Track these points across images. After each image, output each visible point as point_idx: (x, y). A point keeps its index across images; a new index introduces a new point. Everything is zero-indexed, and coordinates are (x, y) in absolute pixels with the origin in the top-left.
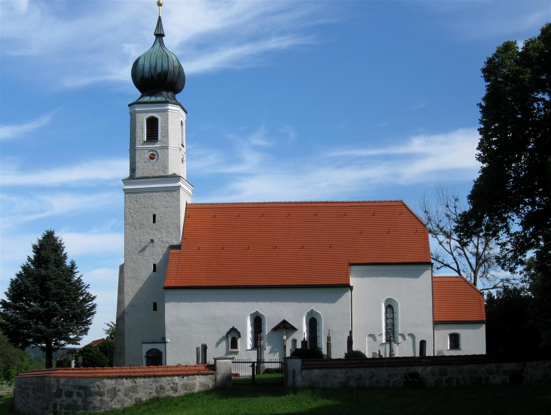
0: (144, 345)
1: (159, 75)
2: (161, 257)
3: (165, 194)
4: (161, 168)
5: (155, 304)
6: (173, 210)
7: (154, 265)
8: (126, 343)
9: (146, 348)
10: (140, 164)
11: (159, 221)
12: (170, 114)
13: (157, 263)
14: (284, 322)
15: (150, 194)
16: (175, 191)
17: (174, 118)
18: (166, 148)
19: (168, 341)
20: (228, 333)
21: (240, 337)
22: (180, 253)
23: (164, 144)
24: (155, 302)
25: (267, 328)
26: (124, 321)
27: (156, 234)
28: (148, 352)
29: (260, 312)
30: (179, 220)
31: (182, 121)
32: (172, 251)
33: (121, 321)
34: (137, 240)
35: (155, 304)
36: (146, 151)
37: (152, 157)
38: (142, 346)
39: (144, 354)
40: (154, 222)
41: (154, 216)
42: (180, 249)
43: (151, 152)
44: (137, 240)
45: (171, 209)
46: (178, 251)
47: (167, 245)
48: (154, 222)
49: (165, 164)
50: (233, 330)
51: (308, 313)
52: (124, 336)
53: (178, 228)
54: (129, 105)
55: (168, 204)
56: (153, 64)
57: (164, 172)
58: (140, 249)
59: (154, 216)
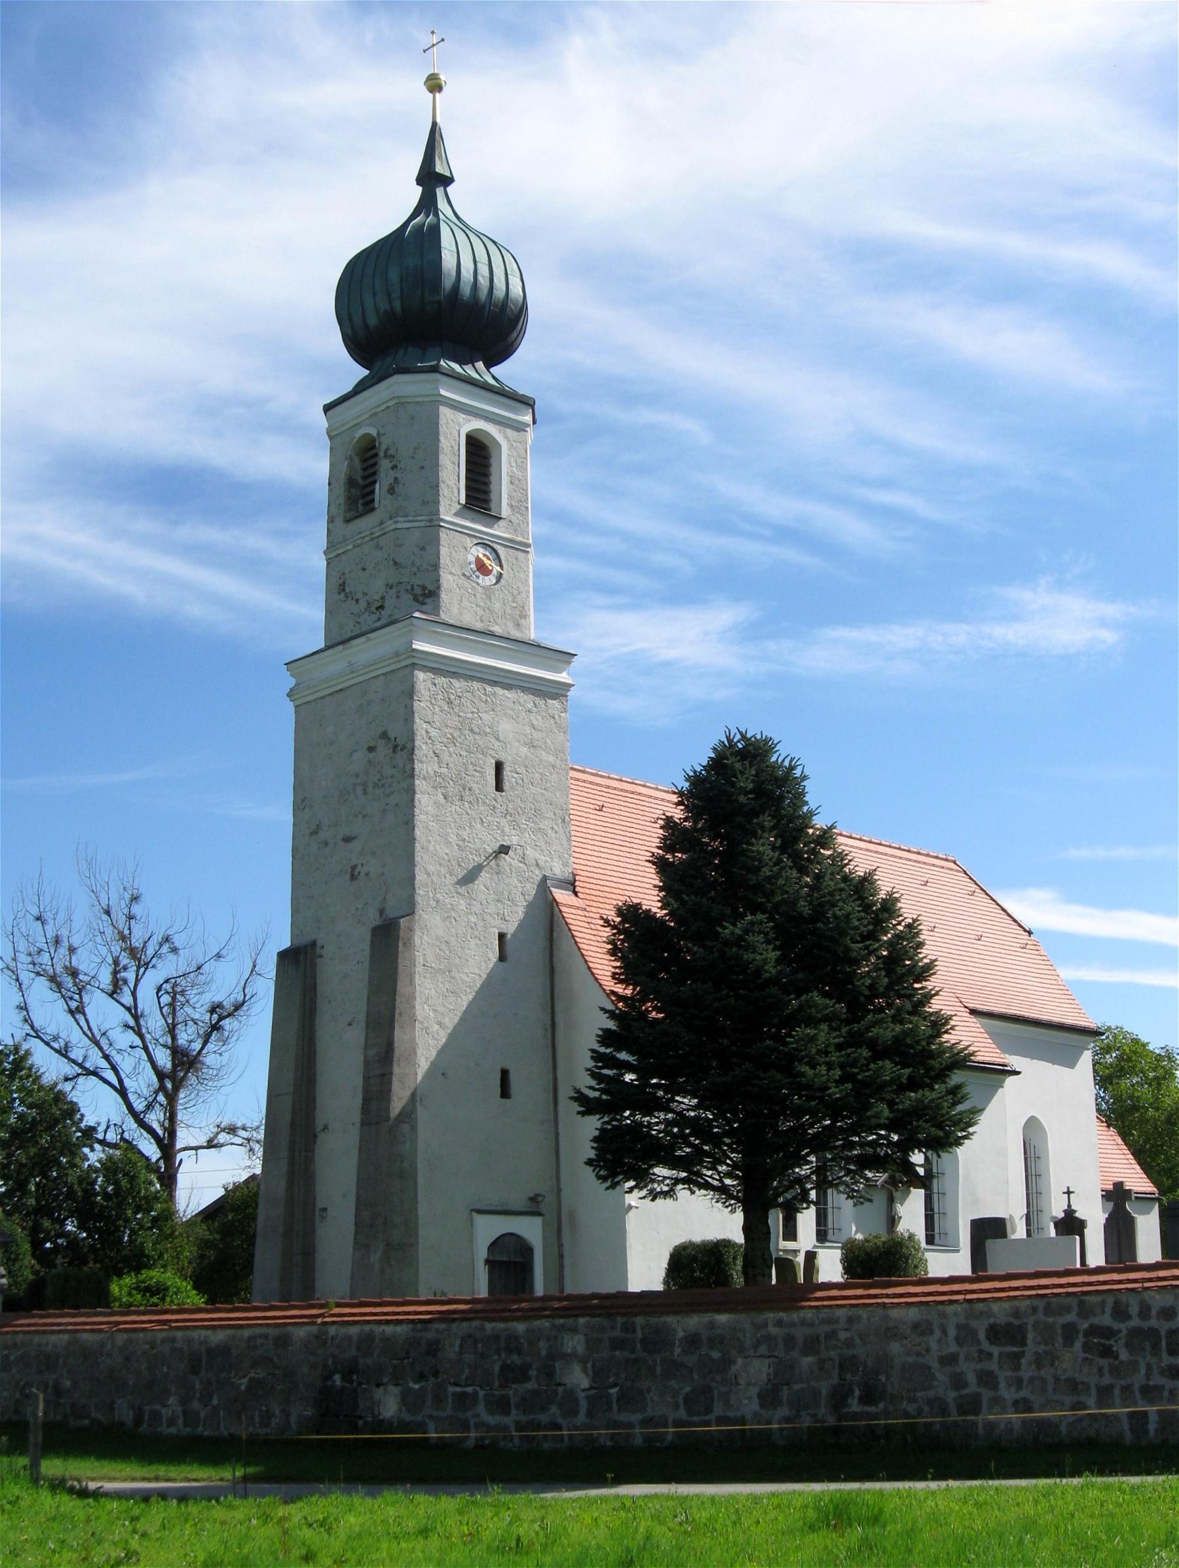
0: (480, 1220)
2: (520, 912)
3: (528, 700)
4: (508, 610)
6: (551, 759)
7: (502, 936)
8: (423, 1210)
9: (488, 1229)
10: (450, 577)
13: (510, 929)
15: (489, 688)
16: (555, 697)
24: (508, 1067)
26: (414, 1128)
27: (507, 830)
28: (494, 1246)
33: (406, 1127)
34: (453, 838)
36: (469, 542)
39: (482, 1253)
40: (499, 787)
41: (499, 767)
44: (453, 838)
48: (499, 787)
52: (416, 1183)
55: (536, 735)
58: (461, 873)
59: (499, 767)
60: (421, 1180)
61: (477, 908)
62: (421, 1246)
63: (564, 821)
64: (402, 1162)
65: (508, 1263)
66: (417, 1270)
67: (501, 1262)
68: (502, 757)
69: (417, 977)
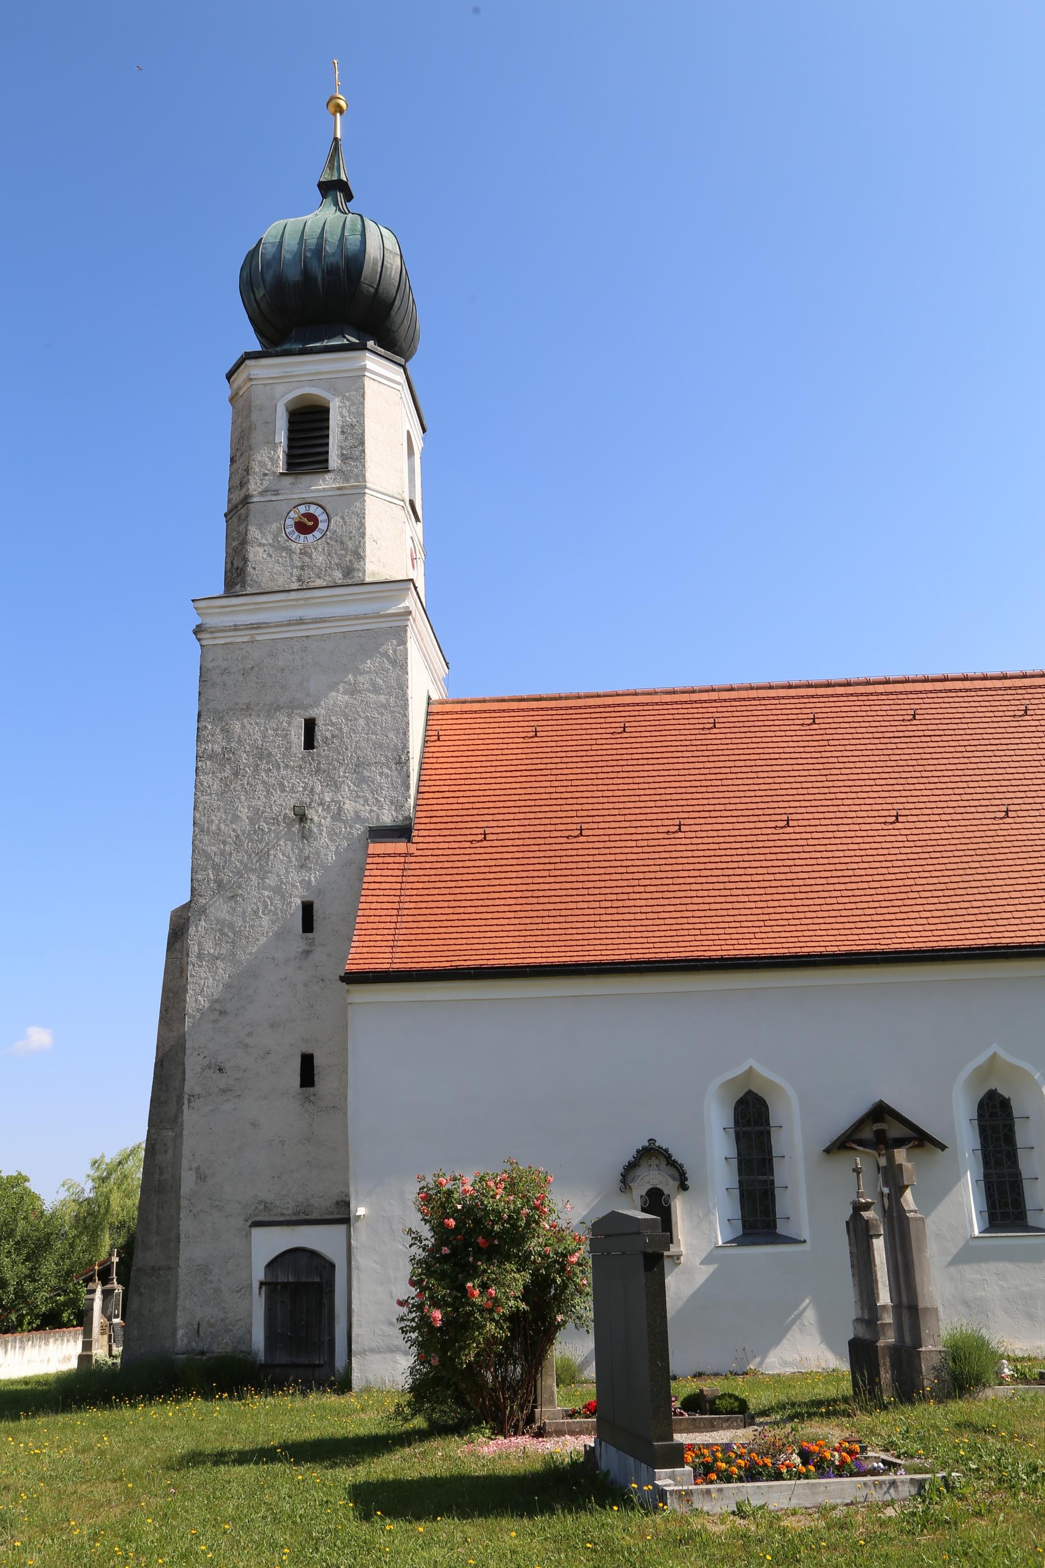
0: (256, 1232)
1: (332, 271)
5: (307, 1062)
6: (382, 698)
9: (269, 1244)
10: (261, 550)
11: (326, 741)
12: (370, 387)
14: (881, 1112)
17: (382, 404)
18: (355, 490)
19: (361, 1211)
20: (631, 1167)
21: (684, 1187)
22: (406, 855)
23: (347, 480)
24: (309, 1050)
25: (797, 1141)
26: (178, 1137)
27: (318, 789)
28: (272, 1265)
29: (763, 1071)
30: (405, 733)
31: (408, 432)
32: (375, 848)
35: (307, 1062)
37: (306, 526)
38: (248, 1235)
39: (259, 1274)
40: (309, 743)
41: (310, 726)
42: (409, 840)
43: (302, 509)
45: (372, 697)
46: (401, 847)
47: (359, 829)
49: (350, 545)
50: (651, 1153)
51: (978, 1070)
53: (402, 762)
54: (229, 376)
56: (312, 242)
57: (348, 572)
59: (310, 726)
60: (185, 1190)
61: (271, 881)
62: (182, 1272)
63: (399, 763)
64: (161, 1173)
65: (298, 1285)
66: (176, 1298)
67: (285, 1285)
68: (311, 713)
69: (190, 967)
